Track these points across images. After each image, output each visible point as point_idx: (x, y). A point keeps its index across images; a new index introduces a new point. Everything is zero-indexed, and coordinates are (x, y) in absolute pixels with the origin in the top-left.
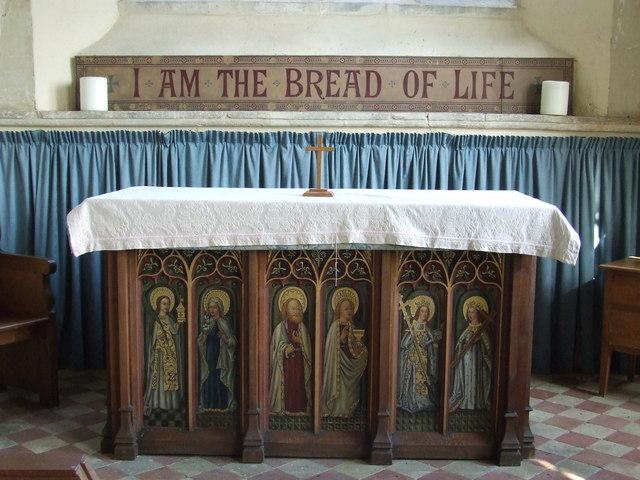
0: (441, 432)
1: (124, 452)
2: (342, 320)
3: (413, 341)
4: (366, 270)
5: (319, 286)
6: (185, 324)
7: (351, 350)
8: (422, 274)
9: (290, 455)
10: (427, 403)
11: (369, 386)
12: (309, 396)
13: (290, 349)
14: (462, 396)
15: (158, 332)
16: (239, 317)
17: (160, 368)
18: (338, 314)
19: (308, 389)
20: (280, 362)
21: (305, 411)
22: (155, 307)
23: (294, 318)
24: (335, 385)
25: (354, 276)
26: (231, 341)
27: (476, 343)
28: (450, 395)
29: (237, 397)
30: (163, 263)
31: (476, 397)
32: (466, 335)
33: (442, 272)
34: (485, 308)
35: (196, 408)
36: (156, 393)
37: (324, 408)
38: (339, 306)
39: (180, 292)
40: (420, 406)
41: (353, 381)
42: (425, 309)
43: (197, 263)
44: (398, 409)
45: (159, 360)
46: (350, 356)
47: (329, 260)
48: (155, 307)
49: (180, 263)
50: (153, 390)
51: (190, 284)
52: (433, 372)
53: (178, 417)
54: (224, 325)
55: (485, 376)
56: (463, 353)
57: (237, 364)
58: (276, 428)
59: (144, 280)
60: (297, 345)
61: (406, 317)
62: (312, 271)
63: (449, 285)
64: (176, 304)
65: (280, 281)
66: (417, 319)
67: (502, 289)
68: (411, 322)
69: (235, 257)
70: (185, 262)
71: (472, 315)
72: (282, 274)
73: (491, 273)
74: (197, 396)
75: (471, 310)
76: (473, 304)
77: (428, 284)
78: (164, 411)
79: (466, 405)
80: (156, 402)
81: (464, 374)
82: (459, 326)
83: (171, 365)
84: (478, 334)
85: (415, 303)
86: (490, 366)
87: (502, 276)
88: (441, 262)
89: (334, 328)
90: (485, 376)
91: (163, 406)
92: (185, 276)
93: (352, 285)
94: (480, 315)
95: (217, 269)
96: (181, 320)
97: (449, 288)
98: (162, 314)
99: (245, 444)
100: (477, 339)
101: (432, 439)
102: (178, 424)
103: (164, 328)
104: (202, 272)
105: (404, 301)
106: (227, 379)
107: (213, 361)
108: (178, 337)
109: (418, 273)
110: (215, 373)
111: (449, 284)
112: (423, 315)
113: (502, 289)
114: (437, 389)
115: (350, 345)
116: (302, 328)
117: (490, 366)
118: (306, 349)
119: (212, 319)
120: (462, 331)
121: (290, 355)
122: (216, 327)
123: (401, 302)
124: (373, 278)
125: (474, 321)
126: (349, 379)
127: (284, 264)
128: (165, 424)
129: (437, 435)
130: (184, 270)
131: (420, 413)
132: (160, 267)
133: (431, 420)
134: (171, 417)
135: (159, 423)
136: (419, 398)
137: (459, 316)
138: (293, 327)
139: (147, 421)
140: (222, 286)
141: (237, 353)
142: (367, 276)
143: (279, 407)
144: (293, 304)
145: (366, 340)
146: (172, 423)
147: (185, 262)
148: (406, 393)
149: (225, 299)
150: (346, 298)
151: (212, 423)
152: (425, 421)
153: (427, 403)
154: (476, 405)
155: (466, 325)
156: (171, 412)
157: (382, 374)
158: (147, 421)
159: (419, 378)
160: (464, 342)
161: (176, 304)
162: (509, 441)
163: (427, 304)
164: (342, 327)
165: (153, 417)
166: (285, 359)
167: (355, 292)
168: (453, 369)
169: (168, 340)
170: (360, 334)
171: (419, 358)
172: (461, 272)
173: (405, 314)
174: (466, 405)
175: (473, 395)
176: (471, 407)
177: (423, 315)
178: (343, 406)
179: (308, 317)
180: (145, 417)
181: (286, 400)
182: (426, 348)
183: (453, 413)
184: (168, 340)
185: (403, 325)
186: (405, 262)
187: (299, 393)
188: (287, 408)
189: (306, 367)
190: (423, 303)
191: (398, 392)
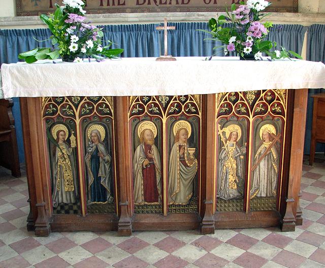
1: (42, 232)
2: (181, 143)
4: (196, 108)
5: (164, 120)
6: (76, 148)
7: (187, 162)
9: (149, 229)
10: (236, 194)
11: (199, 184)
12: (159, 192)
13: (147, 162)
15: (59, 154)
16: (112, 143)
17: (62, 176)
18: (177, 138)
19: (159, 187)
20: (140, 171)
21: (157, 201)
22: (55, 138)
23: (149, 142)
24: (176, 184)
25: (187, 112)
26: (108, 158)
27: (268, 154)
29: (113, 194)
30: (59, 108)
31: (267, 189)
35: (86, 202)
36: (60, 193)
37: (170, 199)
38: (178, 132)
39: (71, 127)
40: (231, 196)
41: (188, 181)
42: (235, 133)
43: (82, 107)
45: (61, 172)
46: (186, 165)
47: (172, 102)
48: (55, 138)
49: (70, 108)
50: (58, 191)
51: (78, 121)
53: (75, 208)
54: (102, 148)
56: (260, 160)
57: (111, 173)
58: (139, 212)
59: (47, 120)
60: (151, 159)
61: (223, 139)
62: (159, 109)
63: (251, 116)
64: (70, 135)
65: (139, 118)
66: (229, 141)
67: (285, 120)
68: (226, 143)
69: (107, 102)
70: (73, 107)
71: (266, 137)
72: (140, 113)
73: (278, 109)
74: (86, 194)
76: (268, 128)
77: (238, 117)
78: (66, 204)
79: (261, 194)
80: (60, 199)
81: (259, 174)
82: (257, 145)
83: (68, 175)
84: (270, 148)
85: (228, 130)
86: (276, 169)
88: (246, 102)
89: (175, 147)
90: (273, 176)
91: (65, 201)
92: (74, 116)
93: (187, 119)
95: (95, 111)
96: (73, 145)
97: (251, 119)
98: (60, 142)
99: (119, 224)
100: (269, 152)
101: (240, 217)
102: (76, 212)
103: (62, 151)
104: (86, 114)
106: (106, 184)
107: (96, 170)
108: (72, 157)
110: (97, 179)
111: (251, 116)
112: (233, 137)
113: (285, 120)
114: (243, 185)
115: (186, 158)
116: (154, 147)
118: (157, 162)
119: (93, 144)
121: (146, 166)
122: (97, 150)
124: (200, 114)
125: (267, 140)
126: (185, 180)
127: (141, 106)
128: (67, 212)
129: (242, 214)
130: (74, 112)
132: (57, 111)
133: (238, 204)
134: (71, 208)
135: (63, 212)
136: (231, 191)
138: (148, 148)
139: (55, 211)
140: (100, 121)
141: (111, 166)
142: (197, 113)
143: (141, 200)
144: (147, 132)
145: (196, 155)
146: (71, 211)
147: (73, 107)
149: (100, 129)
150: (183, 126)
151: (97, 211)
153: (236, 194)
154: (267, 194)
155: (262, 144)
156: (70, 204)
157: (208, 177)
158: (55, 211)
159: (231, 178)
161: (70, 135)
162: (289, 215)
164: (180, 147)
165: (59, 208)
166: (143, 169)
167: (188, 123)
168: (253, 172)
169: (65, 159)
170: (192, 151)
171: (231, 165)
172: (258, 109)
173: (222, 137)
175: (265, 187)
176: (264, 195)
177: (233, 137)
178: (182, 198)
179: (158, 141)
180: (54, 209)
181: (145, 194)
182: (236, 158)
183: (252, 200)
184: (65, 159)
186: (222, 102)
187: (153, 192)
188: (146, 200)
189: (157, 174)
190: (234, 129)
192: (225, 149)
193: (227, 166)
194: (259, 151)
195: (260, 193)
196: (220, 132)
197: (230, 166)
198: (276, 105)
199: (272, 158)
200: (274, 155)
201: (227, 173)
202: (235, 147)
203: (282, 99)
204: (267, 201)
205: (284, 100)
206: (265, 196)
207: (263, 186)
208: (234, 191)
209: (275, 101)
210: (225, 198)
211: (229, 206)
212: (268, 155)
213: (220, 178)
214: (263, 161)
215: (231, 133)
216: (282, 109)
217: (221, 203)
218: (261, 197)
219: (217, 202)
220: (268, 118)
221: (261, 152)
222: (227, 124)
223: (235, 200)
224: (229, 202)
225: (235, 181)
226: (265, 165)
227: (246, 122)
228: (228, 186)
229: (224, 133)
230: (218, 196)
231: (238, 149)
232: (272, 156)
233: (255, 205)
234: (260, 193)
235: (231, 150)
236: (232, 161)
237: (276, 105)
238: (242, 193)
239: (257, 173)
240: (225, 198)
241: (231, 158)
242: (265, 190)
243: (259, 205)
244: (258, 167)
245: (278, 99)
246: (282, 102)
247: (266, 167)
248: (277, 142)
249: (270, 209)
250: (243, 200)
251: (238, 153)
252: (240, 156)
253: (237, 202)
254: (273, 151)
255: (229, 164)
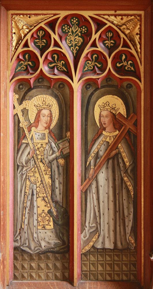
0: (70, 280)
3: (33, 157)
8: (41, 66)
14: (97, 231)
27: (112, 158)
28: (82, 229)
31: (115, 231)
32: (98, 147)
33: (67, 65)
34: (122, 110)
40: (43, 244)
42: (46, 112)
44: (16, 249)
52: (59, 197)
55: (125, 203)
61: (23, 124)
67: (142, 86)
68: (30, 131)
71: (106, 120)
73: (128, 65)
75: (104, 113)
79: (103, 243)
81: (98, 199)
82: (90, 137)
84: (116, 143)
86: (131, 188)
87: (142, 68)
90: (125, 203)
94: (116, 121)
97: (77, 85)
100: (114, 152)
105: (21, 101)
109: (36, 67)
111: (76, 78)
112: (44, 120)
113: (142, 86)
117: (131, 188)
120: (93, 145)
123: (17, 105)
125: (110, 127)
131: (44, 254)
136: (42, 234)
137: (89, 123)
148: (25, 227)
152: (50, 265)
154: (115, 243)
155: (99, 135)
159: (41, 206)
160: (97, 156)
163: (49, 107)
173: (22, 119)
174: (103, 243)
175: (112, 228)
176: (109, 245)
177: (44, 120)
183: (85, 254)
185: (20, 135)
186: (20, 50)
191: (15, 225)
192: (27, 145)
193: (32, 179)
194: (95, 149)
195: (101, 239)
196: (19, 110)
197: (39, 180)
198: (124, 57)
199: (121, 165)
200: (126, 160)
201: (33, 195)
202: (47, 141)
203: (135, 45)
204: (116, 258)
205: (139, 46)
206: (112, 247)
207: (106, 226)
208: (49, 233)
209: (120, 48)
210: (30, 249)
211: (39, 268)
212: (113, 158)
213: (20, 206)
214: (104, 170)
215: (39, 112)
216: (135, 64)
217: (24, 260)
218: (104, 249)
219: (15, 258)
220: (110, 83)
221: (98, 152)
222: (30, 93)
223: (50, 255)
224: (40, 259)
225: (50, 212)
226: (107, 179)
227: (67, 91)
228: (35, 223)
229: (25, 112)
230: (17, 244)
231: (53, 145)
232: (120, 161)
233: (92, 268)
234: (101, 239)
235: (39, 146)
236: (43, 168)
237: (124, 57)
238: (65, 239)
239: (92, 197)
240: (30, 249)
241: (41, 164)
242: (112, 233)
243: (100, 268)
244: (94, 186)
245: (125, 45)
246: (133, 52)
247: (111, 184)
248: (129, 132)
249: (125, 278)
250: (67, 256)
251: (54, 152)
252: (56, 158)
253: (56, 259)
254: (122, 148)
255: (37, 175)
